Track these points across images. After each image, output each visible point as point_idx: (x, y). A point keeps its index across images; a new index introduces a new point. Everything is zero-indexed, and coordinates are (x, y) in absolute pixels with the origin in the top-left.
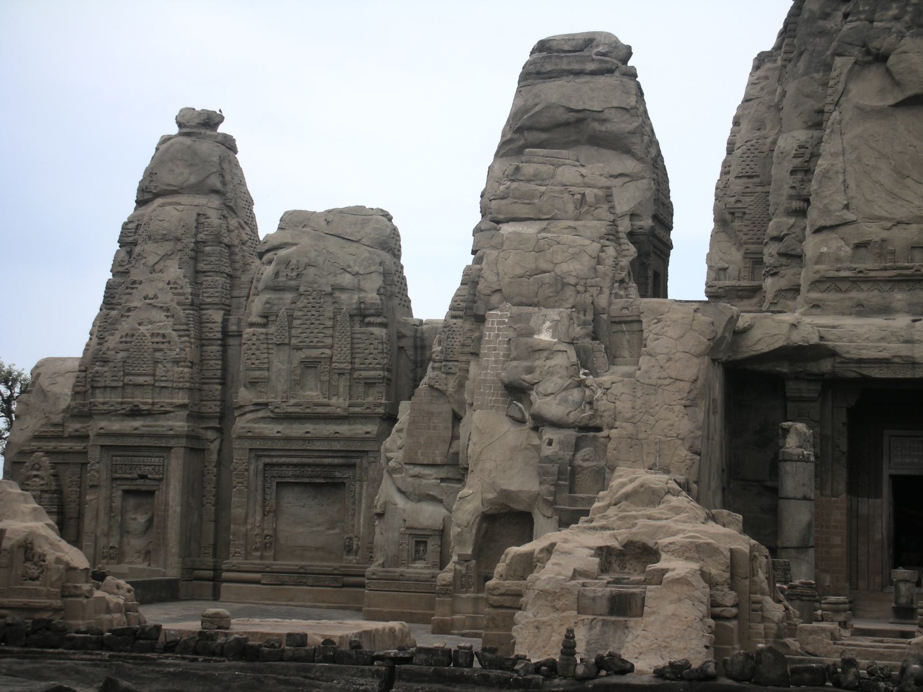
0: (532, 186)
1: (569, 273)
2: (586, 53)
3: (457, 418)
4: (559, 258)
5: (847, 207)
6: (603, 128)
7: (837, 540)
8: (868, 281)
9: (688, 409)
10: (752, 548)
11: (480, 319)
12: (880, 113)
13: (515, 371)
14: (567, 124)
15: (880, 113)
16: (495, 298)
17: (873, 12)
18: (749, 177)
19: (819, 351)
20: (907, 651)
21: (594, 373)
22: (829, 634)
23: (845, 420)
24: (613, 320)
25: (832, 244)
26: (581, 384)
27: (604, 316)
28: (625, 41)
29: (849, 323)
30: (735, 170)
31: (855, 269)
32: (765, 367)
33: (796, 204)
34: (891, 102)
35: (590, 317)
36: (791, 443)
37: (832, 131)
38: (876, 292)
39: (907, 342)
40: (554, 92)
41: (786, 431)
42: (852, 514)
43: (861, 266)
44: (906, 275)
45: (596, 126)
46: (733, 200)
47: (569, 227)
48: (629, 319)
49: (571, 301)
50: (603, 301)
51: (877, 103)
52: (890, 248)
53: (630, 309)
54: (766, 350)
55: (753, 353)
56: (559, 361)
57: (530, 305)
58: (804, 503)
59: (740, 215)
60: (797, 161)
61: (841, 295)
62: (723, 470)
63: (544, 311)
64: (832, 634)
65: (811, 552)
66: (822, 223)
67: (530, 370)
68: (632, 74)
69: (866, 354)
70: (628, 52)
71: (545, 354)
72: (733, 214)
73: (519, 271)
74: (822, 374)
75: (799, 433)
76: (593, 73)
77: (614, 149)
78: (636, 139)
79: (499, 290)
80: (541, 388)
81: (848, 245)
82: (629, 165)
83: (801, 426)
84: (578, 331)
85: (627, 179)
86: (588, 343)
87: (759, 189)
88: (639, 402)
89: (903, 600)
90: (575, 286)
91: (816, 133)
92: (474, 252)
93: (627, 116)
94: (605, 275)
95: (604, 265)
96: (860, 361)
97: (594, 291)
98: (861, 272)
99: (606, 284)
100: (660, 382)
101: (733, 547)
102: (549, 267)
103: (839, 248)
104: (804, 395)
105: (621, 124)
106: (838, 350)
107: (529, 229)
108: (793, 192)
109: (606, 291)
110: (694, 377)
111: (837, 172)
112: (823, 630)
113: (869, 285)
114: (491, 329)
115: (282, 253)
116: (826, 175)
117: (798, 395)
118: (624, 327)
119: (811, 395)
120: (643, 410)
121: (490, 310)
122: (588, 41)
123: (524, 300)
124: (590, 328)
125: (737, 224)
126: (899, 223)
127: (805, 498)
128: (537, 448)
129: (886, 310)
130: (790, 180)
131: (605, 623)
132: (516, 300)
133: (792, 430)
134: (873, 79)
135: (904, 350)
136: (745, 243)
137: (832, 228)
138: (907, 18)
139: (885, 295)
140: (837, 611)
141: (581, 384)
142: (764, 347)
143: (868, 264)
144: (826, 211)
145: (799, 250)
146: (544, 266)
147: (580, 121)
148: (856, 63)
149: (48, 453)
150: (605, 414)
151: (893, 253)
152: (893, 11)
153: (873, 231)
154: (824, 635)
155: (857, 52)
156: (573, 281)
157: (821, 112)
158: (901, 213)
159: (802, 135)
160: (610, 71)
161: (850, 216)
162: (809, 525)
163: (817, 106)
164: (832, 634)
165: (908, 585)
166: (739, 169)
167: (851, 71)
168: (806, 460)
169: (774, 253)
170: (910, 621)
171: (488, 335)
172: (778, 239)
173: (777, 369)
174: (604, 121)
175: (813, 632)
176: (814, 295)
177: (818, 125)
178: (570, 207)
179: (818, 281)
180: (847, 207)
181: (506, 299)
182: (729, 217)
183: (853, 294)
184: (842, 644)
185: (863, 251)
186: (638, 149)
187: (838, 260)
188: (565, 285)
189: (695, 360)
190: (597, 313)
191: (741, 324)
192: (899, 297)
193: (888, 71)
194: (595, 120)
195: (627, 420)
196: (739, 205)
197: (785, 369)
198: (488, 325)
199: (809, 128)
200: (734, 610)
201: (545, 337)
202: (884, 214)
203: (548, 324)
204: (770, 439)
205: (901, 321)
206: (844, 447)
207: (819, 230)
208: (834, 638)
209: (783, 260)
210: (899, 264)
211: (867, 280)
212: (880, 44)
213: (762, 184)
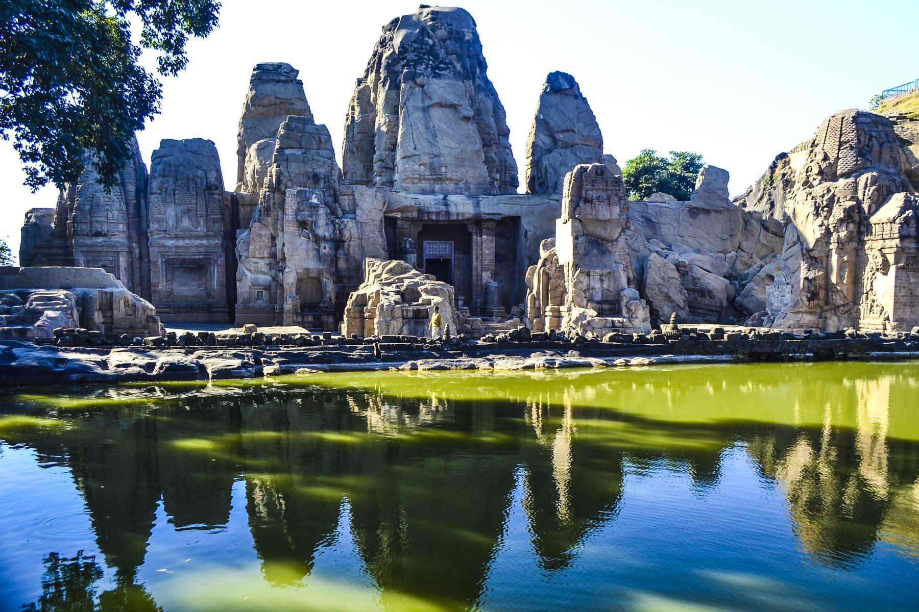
3: (273, 238)
4: (315, 166)
11: (284, 193)
14: (275, 104)
16: (289, 184)
21: (337, 217)
29: (421, 197)
40: (269, 88)
68: (300, 83)
76: (284, 82)
107: (298, 152)
115: (165, 159)
122: (280, 66)
128: (318, 251)
129: (433, 192)
131: (415, 322)
137: (410, 157)
145: (391, 166)
149: (45, 255)
161: (417, 153)
171: (288, 200)
172: (383, 161)
174: (291, 104)
180: (415, 148)
188: (319, 178)
190: (335, 190)
197: (399, 215)
201: (314, 201)
211: (425, 179)
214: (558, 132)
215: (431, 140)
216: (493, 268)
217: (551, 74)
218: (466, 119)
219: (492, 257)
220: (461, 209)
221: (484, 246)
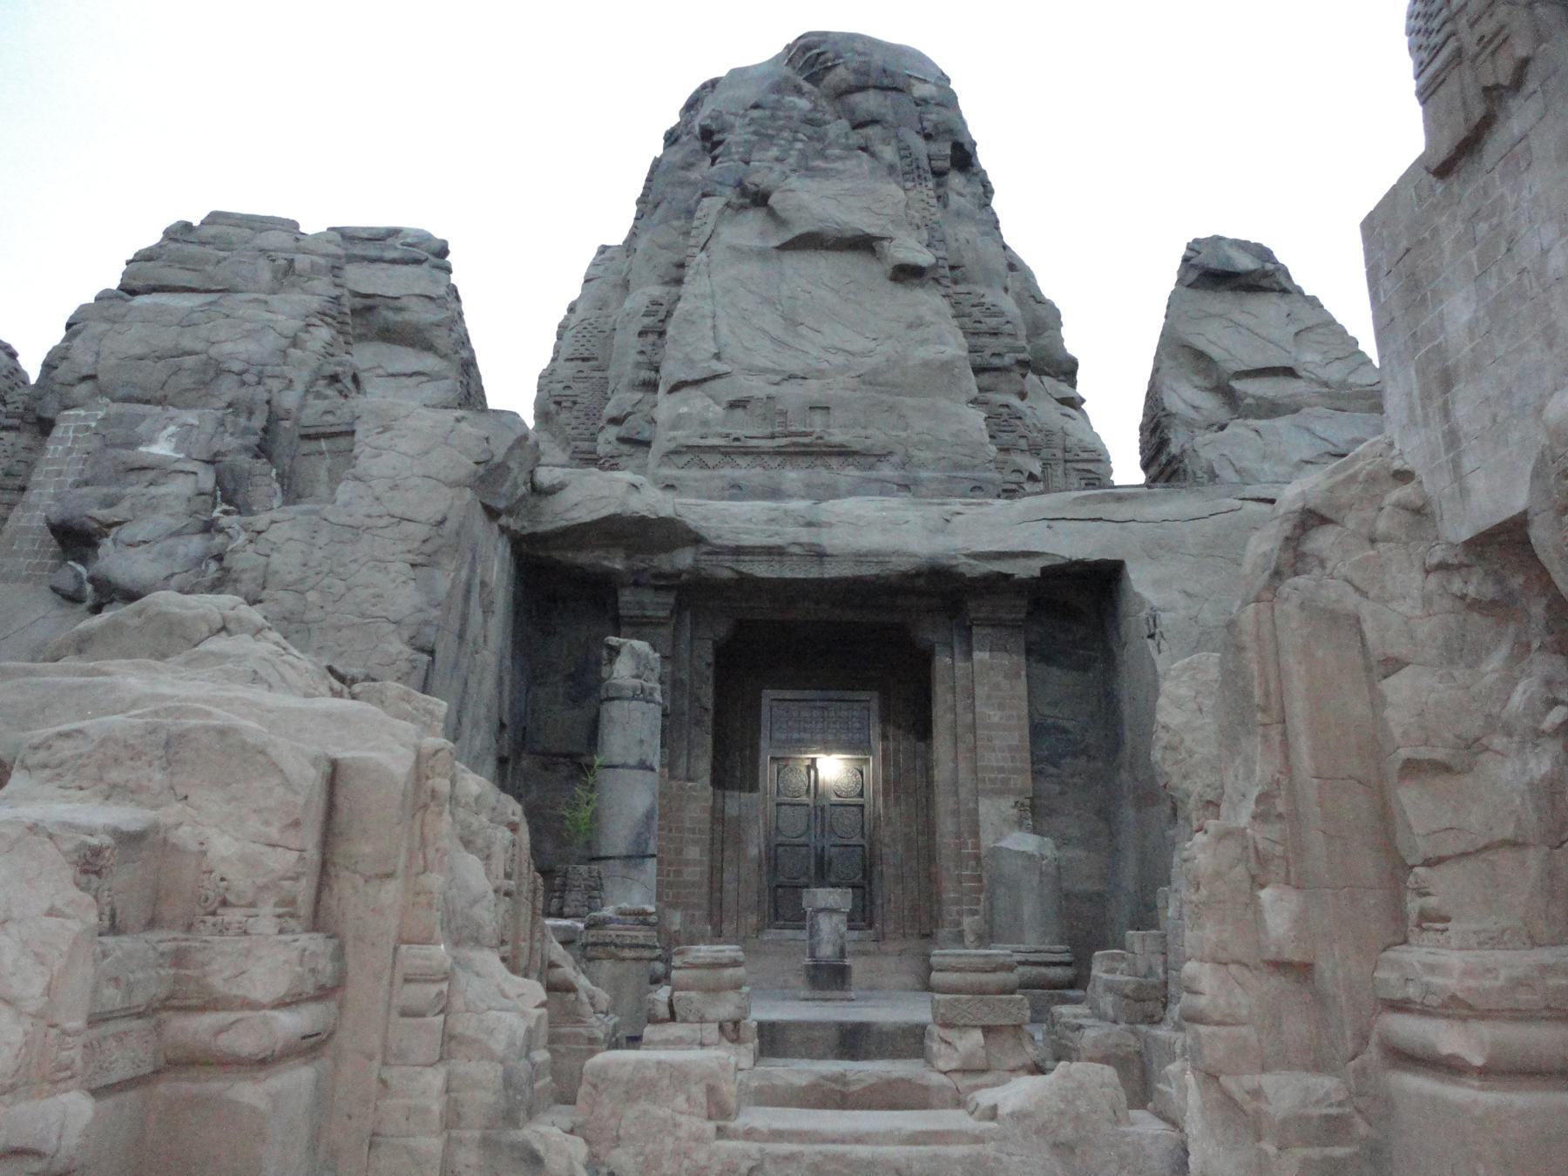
0: (208, 249)
1: (232, 356)
2: (389, 241)
4: (222, 335)
5: (717, 356)
6: (399, 318)
7: (693, 852)
8: (746, 454)
9: (419, 570)
10: (422, 764)
12: (762, 255)
13: (88, 507)
15: (762, 255)
16: (83, 389)
17: (750, 152)
18: (584, 360)
19: (671, 533)
20: (989, 1149)
21: (243, 509)
22: (698, 1092)
23: (710, 659)
24: (304, 432)
25: (694, 403)
26: (209, 527)
27: (287, 424)
28: (439, 235)
30: (566, 352)
31: (727, 436)
32: (584, 558)
33: (646, 374)
34: (777, 243)
35: (259, 422)
36: (622, 671)
37: (697, 273)
38: (759, 470)
39: (810, 524)
41: (615, 651)
42: (718, 816)
43: (739, 433)
44: (804, 445)
45: (390, 315)
46: (561, 386)
47: (256, 300)
48: (333, 429)
49: (227, 398)
50: (289, 400)
51: (757, 243)
52: (779, 407)
53: (339, 412)
54: (588, 519)
55: (564, 523)
56: (181, 487)
57: (148, 402)
58: (639, 774)
59: (569, 404)
60: (647, 321)
61: (707, 473)
62: (502, 726)
63: (172, 411)
64: (711, 1090)
65: (651, 865)
66: (683, 377)
67: (110, 503)
69: (747, 540)
70: (443, 251)
71: (151, 475)
72: (558, 403)
73: (138, 350)
74: (678, 574)
75: (635, 654)
76: (394, 261)
77: (412, 346)
78: (443, 332)
79: (92, 377)
80: (126, 533)
81: (718, 404)
82: (429, 362)
83: (641, 646)
84: (229, 442)
85: (424, 379)
86: (245, 461)
87: (597, 374)
88: (318, 554)
89: (826, 951)
90: (240, 374)
91: (674, 290)
92: (69, 326)
93: (431, 306)
94: (302, 363)
95: (303, 349)
96: (738, 551)
97: (275, 385)
98: (737, 439)
99: (301, 377)
100: (368, 522)
101: (339, 756)
102: (199, 346)
103: (707, 408)
104: (649, 613)
105: (422, 314)
106: (703, 533)
108: (641, 358)
109: (299, 387)
110: (439, 517)
111: (703, 317)
112: (680, 1076)
113: (749, 459)
114: (61, 440)
116: (688, 320)
117: (637, 612)
118: (324, 444)
119: (661, 614)
120: (325, 569)
121: (67, 408)
122: (394, 232)
123: (137, 393)
124: (253, 440)
125: (564, 416)
126: (791, 377)
127: (643, 766)
130: (636, 344)
132: (120, 393)
133: (624, 650)
134: (753, 220)
135: (805, 536)
136: (574, 440)
137: (696, 383)
138: (792, 160)
139: (772, 473)
140: (715, 990)
141: (209, 527)
142: (584, 515)
143: (747, 427)
144: (689, 362)
145: (646, 435)
146: (187, 343)
147: (370, 309)
148: (728, 205)
150: (245, 576)
151: (783, 413)
152: (774, 152)
153: (757, 387)
154: (680, 1101)
155: (730, 194)
156: (237, 366)
157: (681, 265)
158: (792, 364)
159: (657, 291)
160: (418, 262)
162: (649, 816)
163: (676, 258)
164: (711, 1090)
165: (836, 918)
166: (571, 350)
167: (721, 213)
168: (643, 695)
169: (612, 439)
170: (837, 994)
173: (606, 563)
175: (640, 1088)
176: (666, 471)
177: (679, 281)
178: (266, 276)
179: (675, 452)
180: (717, 356)
181: (102, 392)
182: (553, 407)
183: (727, 471)
184: (749, 1134)
185: (739, 413)
186: (442, 340)
187: (705, 423)
188: (220, 372)
189: (447, 490)
190: (273, 419)
191: (545, 476)
192: (792, 476)
193: (772, 214)
194: (389, 308)
195: (286, 588)
196: (568, 392)
197: (617, 563)
198: (57, 432)
199: (666, 283)
200: (292, 1023)
201: (162, 449)
202: (770, 365)
203: (172, 429)
204: (587, 688)
205: (798, 505)
206: (709, 704)
207: (676, 387)
208: (718, 1109)
209: (625, 448)
210: (793, 429)
211: (747, 452)
212: (760, 177)
213: (598, 369)
214: (1240, 375)
215: (777, 330)
216: (1023, 781)
217: (1196, 241)
218: (907, 274)
219: (1018, 735)
220: (873, 540)
221: (981, 691)
